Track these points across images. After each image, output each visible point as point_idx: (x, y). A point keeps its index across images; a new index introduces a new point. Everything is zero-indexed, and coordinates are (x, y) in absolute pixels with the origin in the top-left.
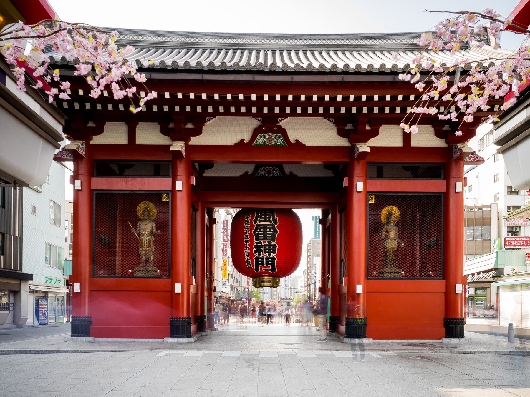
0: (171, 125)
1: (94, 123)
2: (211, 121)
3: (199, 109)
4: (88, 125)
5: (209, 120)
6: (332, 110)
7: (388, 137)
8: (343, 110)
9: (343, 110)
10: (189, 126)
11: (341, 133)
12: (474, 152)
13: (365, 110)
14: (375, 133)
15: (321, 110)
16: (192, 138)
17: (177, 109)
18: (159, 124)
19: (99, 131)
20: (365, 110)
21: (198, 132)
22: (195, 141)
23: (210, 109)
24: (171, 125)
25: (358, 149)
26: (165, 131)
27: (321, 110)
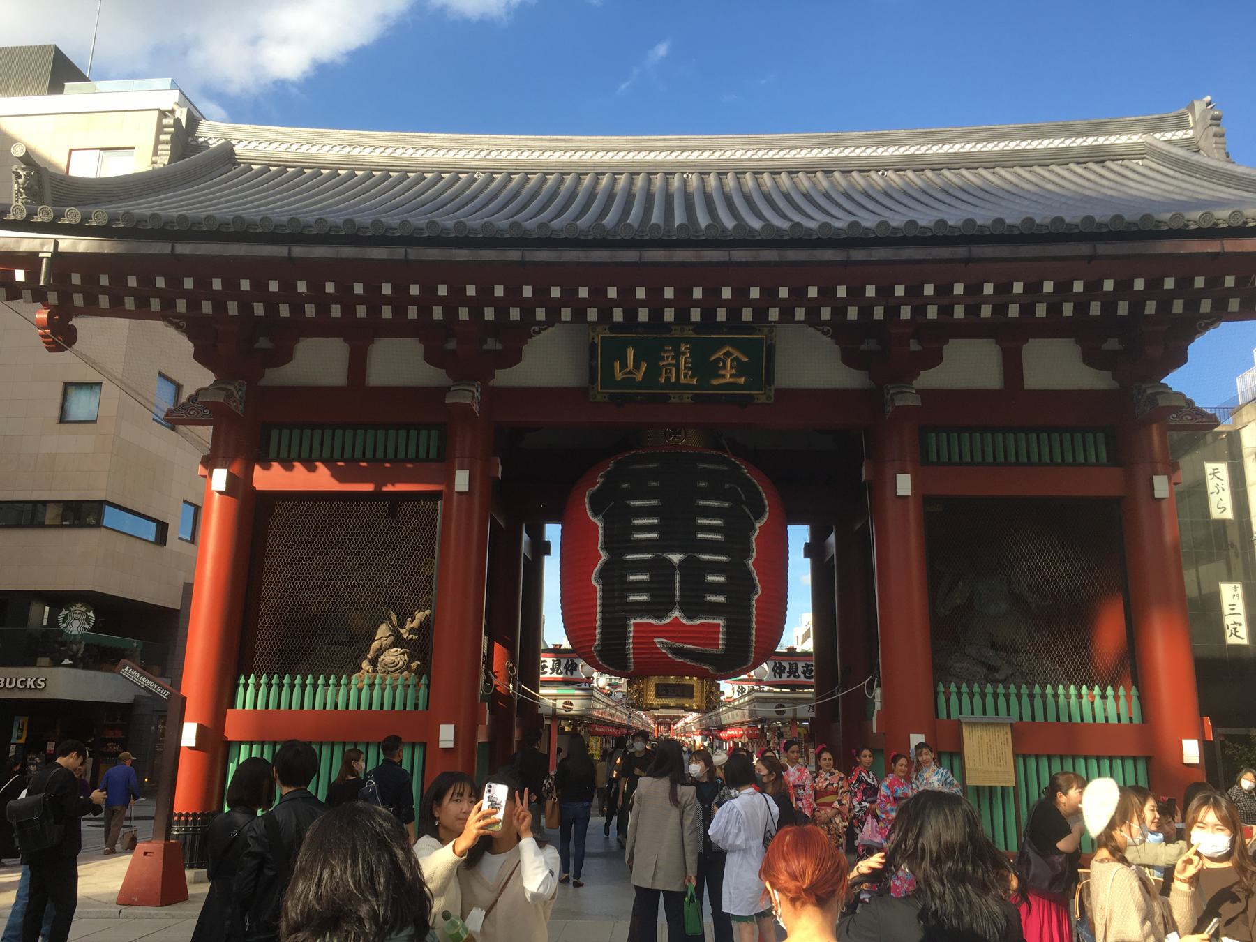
0: (452, 345)
3: (515, 314)
4: (257, 346)
5: (538, 333)
6: (826, 313)
8: (852, 313)
9: (852, 313)
10: (492, 344)
11: (850, 358)
12: (1190, 403)
13: (906, 313)
14: (934, 359)
15: (800, 314)
16: (497, 372)
17: (464, 313)
18: (420, 341)
20: (906, 313)
21: (512, 357)
22: (505, 378)
23: (541, 314)
24: (452, 345)
25: (892, 400)
27: (800, 314)
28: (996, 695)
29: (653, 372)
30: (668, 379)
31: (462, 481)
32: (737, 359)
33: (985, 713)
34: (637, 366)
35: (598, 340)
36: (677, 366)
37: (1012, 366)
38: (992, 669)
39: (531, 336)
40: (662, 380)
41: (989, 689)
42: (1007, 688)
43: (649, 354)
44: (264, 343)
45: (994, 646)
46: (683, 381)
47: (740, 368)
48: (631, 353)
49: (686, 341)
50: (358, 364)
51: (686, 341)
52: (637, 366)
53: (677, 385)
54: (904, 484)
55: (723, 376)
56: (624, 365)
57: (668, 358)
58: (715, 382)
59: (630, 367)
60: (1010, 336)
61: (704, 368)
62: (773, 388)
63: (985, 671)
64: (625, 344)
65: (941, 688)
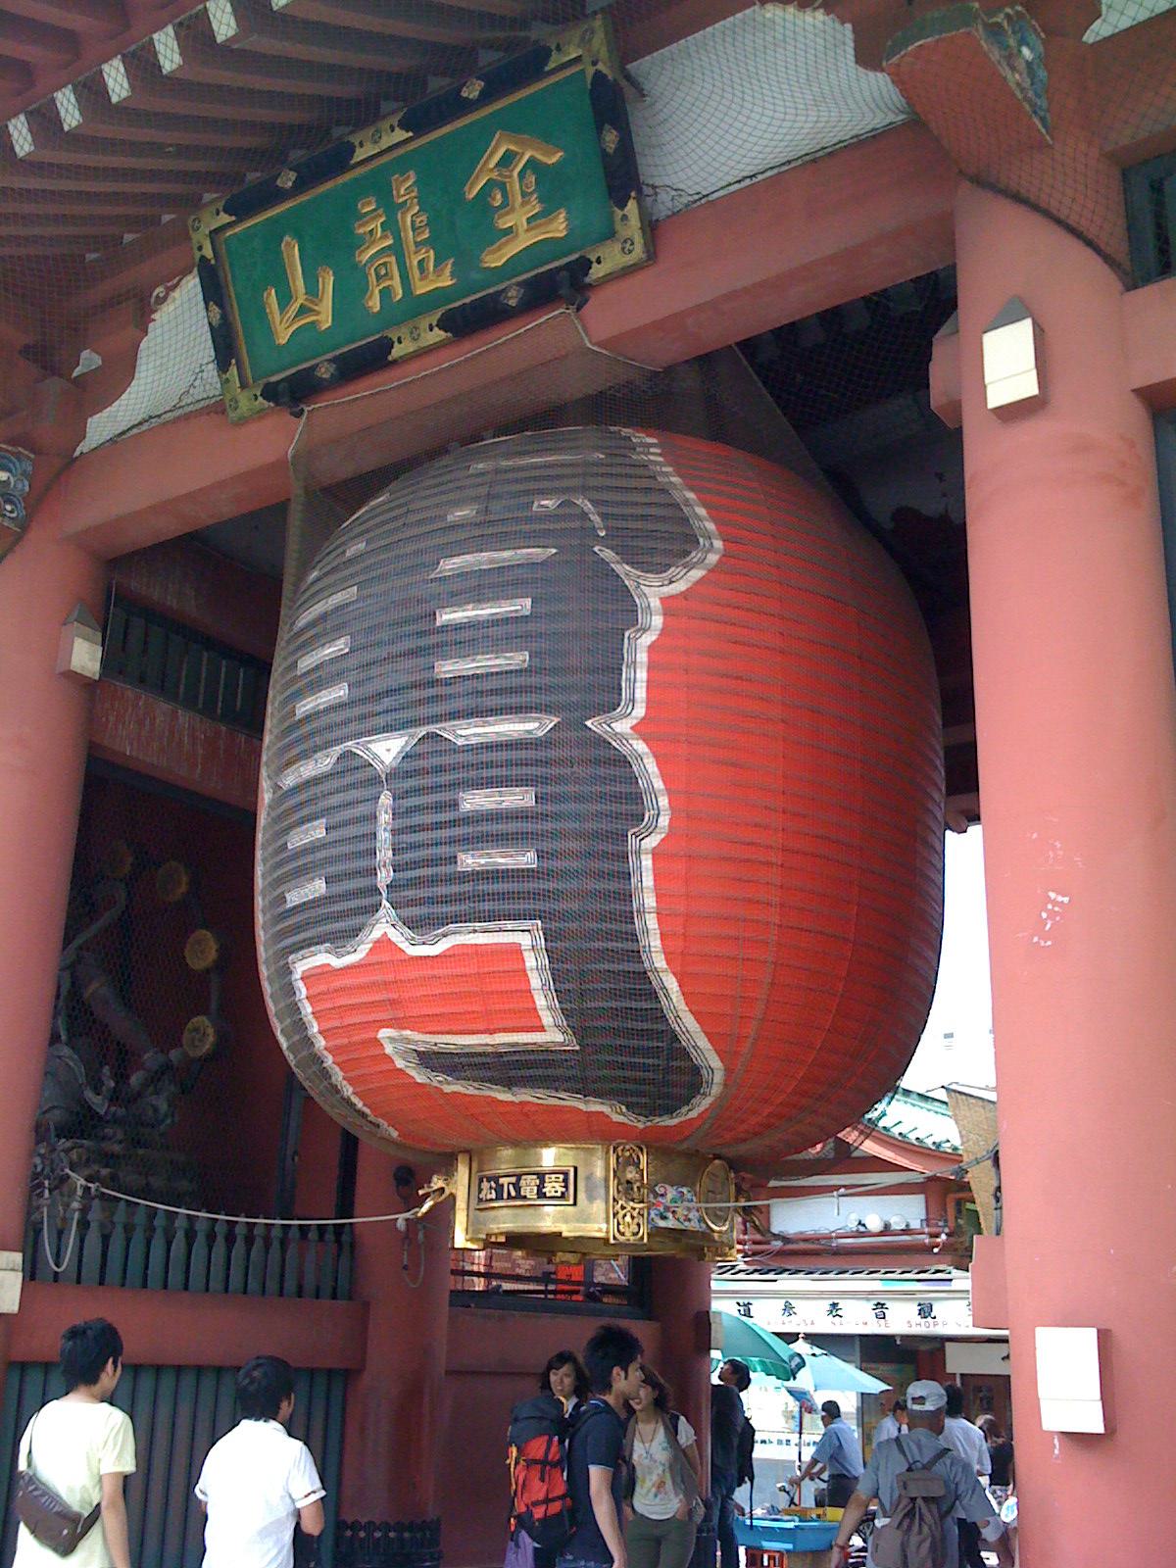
2: (176, 294)
30: (386, 294)
36: (398, 250)
40: (375, 304)
43: (334, 245)
46: (421, 288)
51: (402, 166)
52: (313, 291)
56: (285, 298)
61: (461, 226)
64: (274, 234)
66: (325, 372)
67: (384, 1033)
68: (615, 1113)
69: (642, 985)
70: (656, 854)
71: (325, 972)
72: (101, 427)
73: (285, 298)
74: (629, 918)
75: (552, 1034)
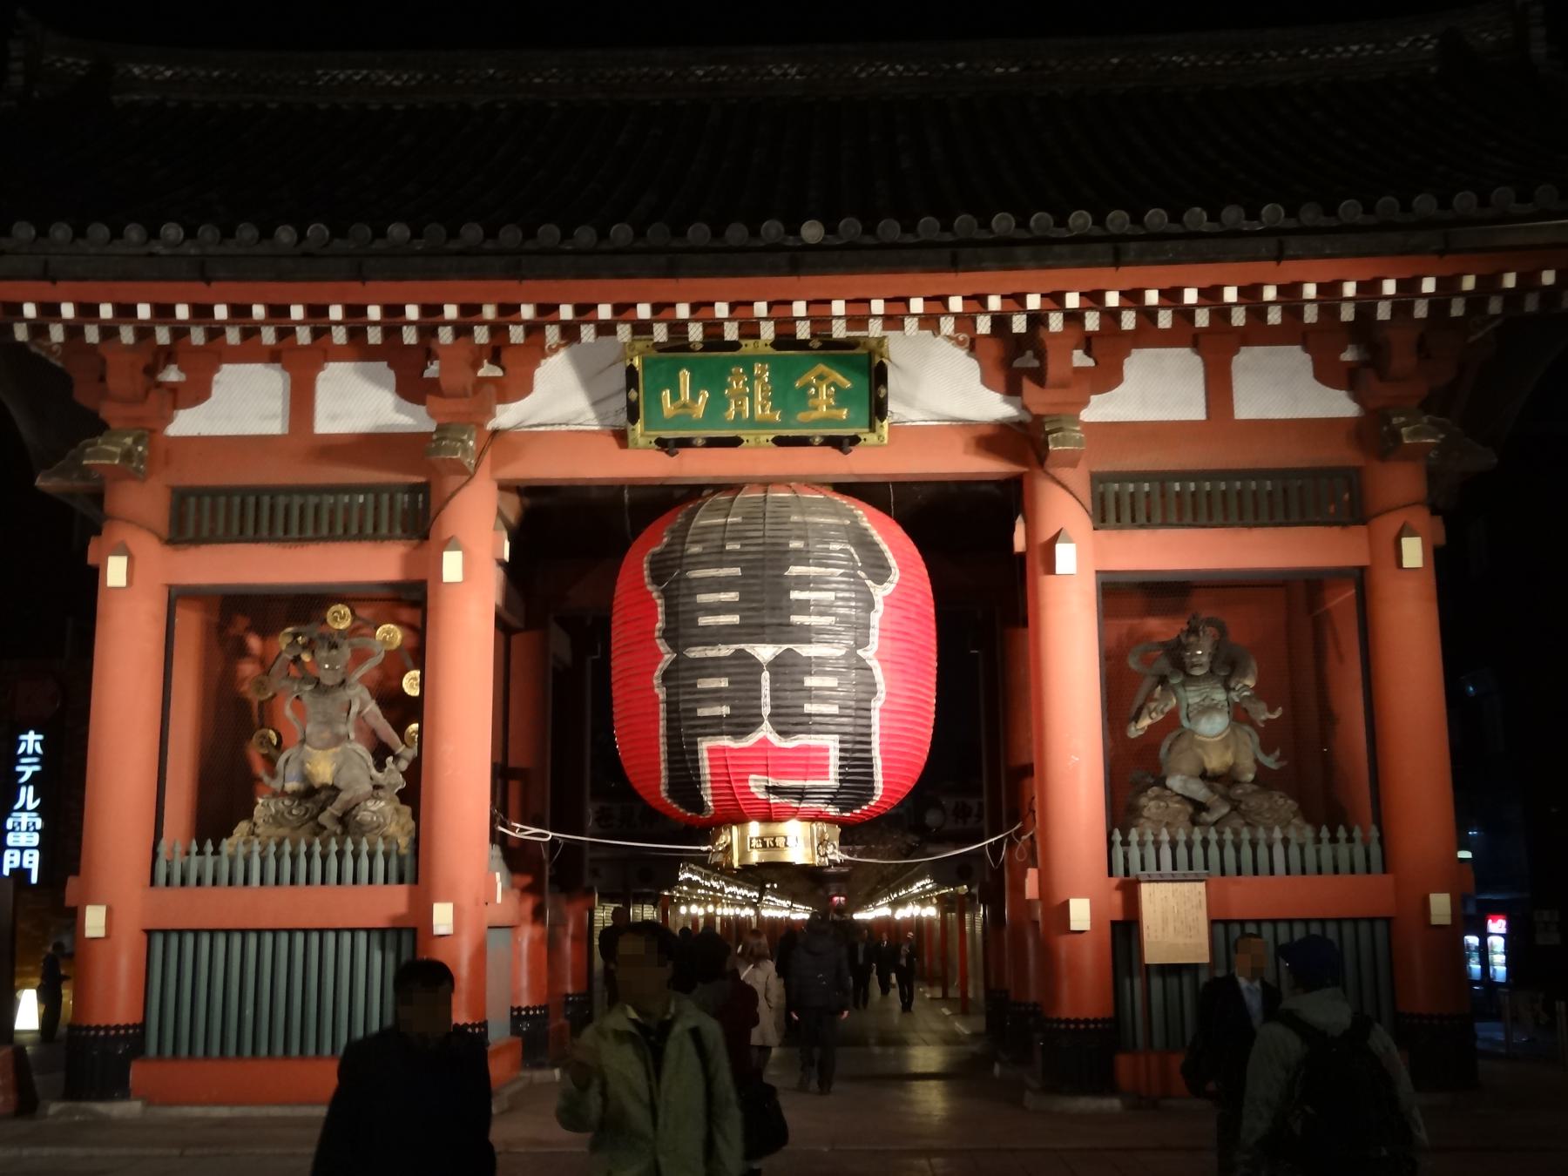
1: (181, 369)
6: (947, 325)
7: (1156, 391)
16: (499, 408)
18: (391, 366)
19: (197, 392)
26: (412, 389)
28: (1205, 843)
29: (717, 405)
30: (739, 414)
31: (452, 566)
32: (833, 384)
33: (1174, 868)
34: (694, 397)
35: (637, 362)
36: (752, 396)
37: (1218, 387)
38: (1199, 807)
39: (544, 356)
41: (1197, 835)
42: (1220, 833)
43: (711, 379)
44: (172, 375)
45: (1204, 776)
47: (842, 397)
48: (685, 376)
49: (763, 359)
50: (301, 401)
51: (763, 359)
52: (694, 397)
53: (755, 424)
54: (1066, 557)
55: (816, 409)
56: (675, 396)
57: (737, 385)
58: (801, 416)
59: (684, 399)
60: (1216, 347)
61: (788, 396)
62: (885, 423)
63: (1190, 809)
65: (1117, 837)
66: (700, 442)
67: (752, 777)
68: (832, 811)
69: (868, 763)
70: (882, 710)
71: (724, 749)
72: (507, 416)
73: (675, 396)
74: (869, 735)
75: (832, 780)
